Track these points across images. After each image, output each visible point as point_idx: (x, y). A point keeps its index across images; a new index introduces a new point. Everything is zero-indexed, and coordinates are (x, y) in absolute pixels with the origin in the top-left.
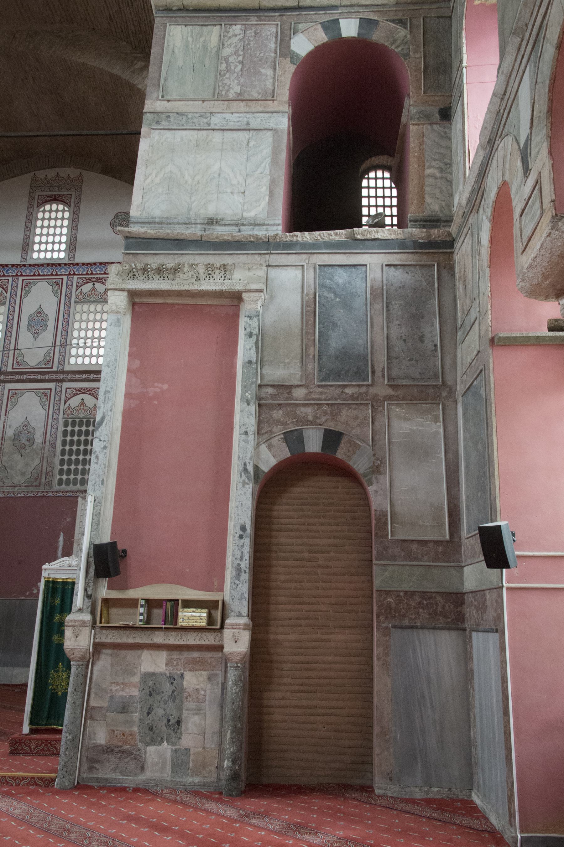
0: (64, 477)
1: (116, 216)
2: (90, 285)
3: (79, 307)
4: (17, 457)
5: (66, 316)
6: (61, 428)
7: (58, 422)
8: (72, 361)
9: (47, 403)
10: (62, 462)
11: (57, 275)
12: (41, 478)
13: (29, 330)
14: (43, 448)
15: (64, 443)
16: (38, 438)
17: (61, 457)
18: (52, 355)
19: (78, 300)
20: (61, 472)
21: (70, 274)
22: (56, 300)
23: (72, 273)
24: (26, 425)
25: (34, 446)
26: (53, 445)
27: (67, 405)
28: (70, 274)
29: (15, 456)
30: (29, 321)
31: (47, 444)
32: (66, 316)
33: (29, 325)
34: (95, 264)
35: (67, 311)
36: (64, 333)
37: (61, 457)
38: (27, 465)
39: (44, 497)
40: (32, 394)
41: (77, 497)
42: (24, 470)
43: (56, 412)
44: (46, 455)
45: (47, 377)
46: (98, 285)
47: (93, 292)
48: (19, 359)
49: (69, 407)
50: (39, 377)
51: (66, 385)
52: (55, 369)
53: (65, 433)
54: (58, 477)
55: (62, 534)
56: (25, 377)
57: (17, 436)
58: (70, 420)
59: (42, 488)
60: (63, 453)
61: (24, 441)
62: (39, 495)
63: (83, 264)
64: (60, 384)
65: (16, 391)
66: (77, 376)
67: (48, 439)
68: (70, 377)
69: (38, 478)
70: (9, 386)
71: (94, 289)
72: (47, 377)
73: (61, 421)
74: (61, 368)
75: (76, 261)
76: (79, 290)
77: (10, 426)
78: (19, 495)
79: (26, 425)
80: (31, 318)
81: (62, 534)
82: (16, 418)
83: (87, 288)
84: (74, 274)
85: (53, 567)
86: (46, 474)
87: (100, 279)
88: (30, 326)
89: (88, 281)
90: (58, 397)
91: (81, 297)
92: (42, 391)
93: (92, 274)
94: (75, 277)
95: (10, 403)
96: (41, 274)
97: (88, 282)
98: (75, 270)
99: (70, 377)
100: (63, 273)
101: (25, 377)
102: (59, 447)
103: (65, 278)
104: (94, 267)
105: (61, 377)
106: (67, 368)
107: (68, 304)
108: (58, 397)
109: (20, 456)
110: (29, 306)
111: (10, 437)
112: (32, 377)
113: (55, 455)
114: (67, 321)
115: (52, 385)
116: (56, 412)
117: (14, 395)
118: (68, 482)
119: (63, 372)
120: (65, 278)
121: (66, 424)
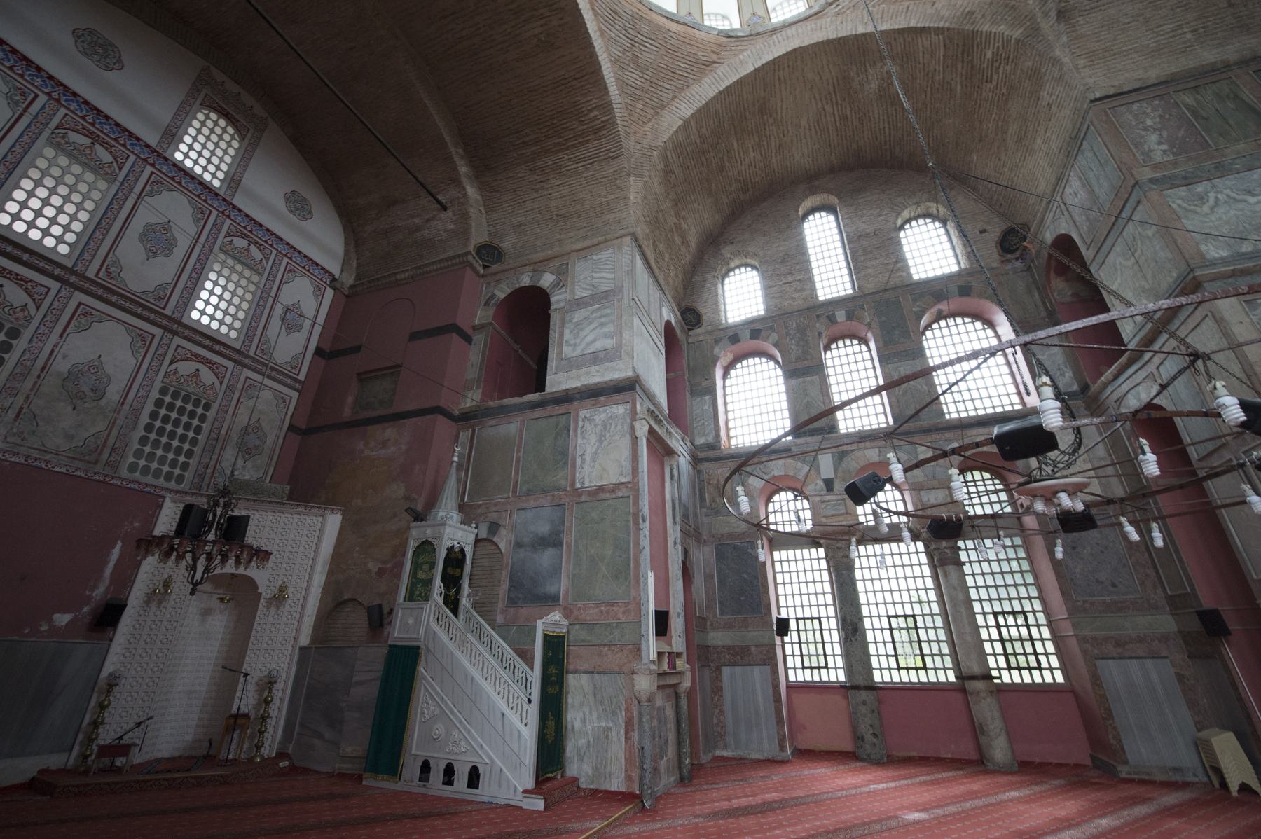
0: (142, 462)
1: (293, 192)
2: (245, 243)
6: (155, 394)
8: (195, 315)
9: (143, 351)
10: (144, 440)
11: (205, 201)
12: (100, 454)
15: (154, 415)
16: (113, 393)
17: (143, 433)
20: (139, 454)
21: (222, 212)
24: (96, 366)
26: (136, 413)
27: (173, 367)
28: (222, 212)
31: (126, 407)
34: (261, 225)
37: (143, 433)
39: (104, 482)
40: (122, 328)
45: (152, 316)
46: (253, 248)
49: (175, 371)
50: (139, 310)
51: (177, 340)
52: (168, 312)
53: (159, 403)
55: (119, 544)
56: (115, 299)
58: (172, 389)
59: (99, 468)
60: (149, 428)
61: (84, 388)
62: (96, 477)
63: (247, 216)
68: (187, 333)
70: (79, 296)
71: (248, 249)
73: (158, 384)
78: (57, 469)
79: (96, 366)
81: (119, 544)
83: (240, 243)
84: (229, 217)
86: (113, 449)
89: (243, 236)
90: (161, 351)
94: (228, 222)
95: (74, 322)
99: (187, 333)
102: (145, 419)
105: (175, 327)
106: (185, 320)
108: (161, 351)
109: (70, 408)
113: (135, 427)
115: (157, 331)
117: (82, 313)
118: (146, 471)
119: (179, 323)
120: (215, 213)
121: (163, 391)
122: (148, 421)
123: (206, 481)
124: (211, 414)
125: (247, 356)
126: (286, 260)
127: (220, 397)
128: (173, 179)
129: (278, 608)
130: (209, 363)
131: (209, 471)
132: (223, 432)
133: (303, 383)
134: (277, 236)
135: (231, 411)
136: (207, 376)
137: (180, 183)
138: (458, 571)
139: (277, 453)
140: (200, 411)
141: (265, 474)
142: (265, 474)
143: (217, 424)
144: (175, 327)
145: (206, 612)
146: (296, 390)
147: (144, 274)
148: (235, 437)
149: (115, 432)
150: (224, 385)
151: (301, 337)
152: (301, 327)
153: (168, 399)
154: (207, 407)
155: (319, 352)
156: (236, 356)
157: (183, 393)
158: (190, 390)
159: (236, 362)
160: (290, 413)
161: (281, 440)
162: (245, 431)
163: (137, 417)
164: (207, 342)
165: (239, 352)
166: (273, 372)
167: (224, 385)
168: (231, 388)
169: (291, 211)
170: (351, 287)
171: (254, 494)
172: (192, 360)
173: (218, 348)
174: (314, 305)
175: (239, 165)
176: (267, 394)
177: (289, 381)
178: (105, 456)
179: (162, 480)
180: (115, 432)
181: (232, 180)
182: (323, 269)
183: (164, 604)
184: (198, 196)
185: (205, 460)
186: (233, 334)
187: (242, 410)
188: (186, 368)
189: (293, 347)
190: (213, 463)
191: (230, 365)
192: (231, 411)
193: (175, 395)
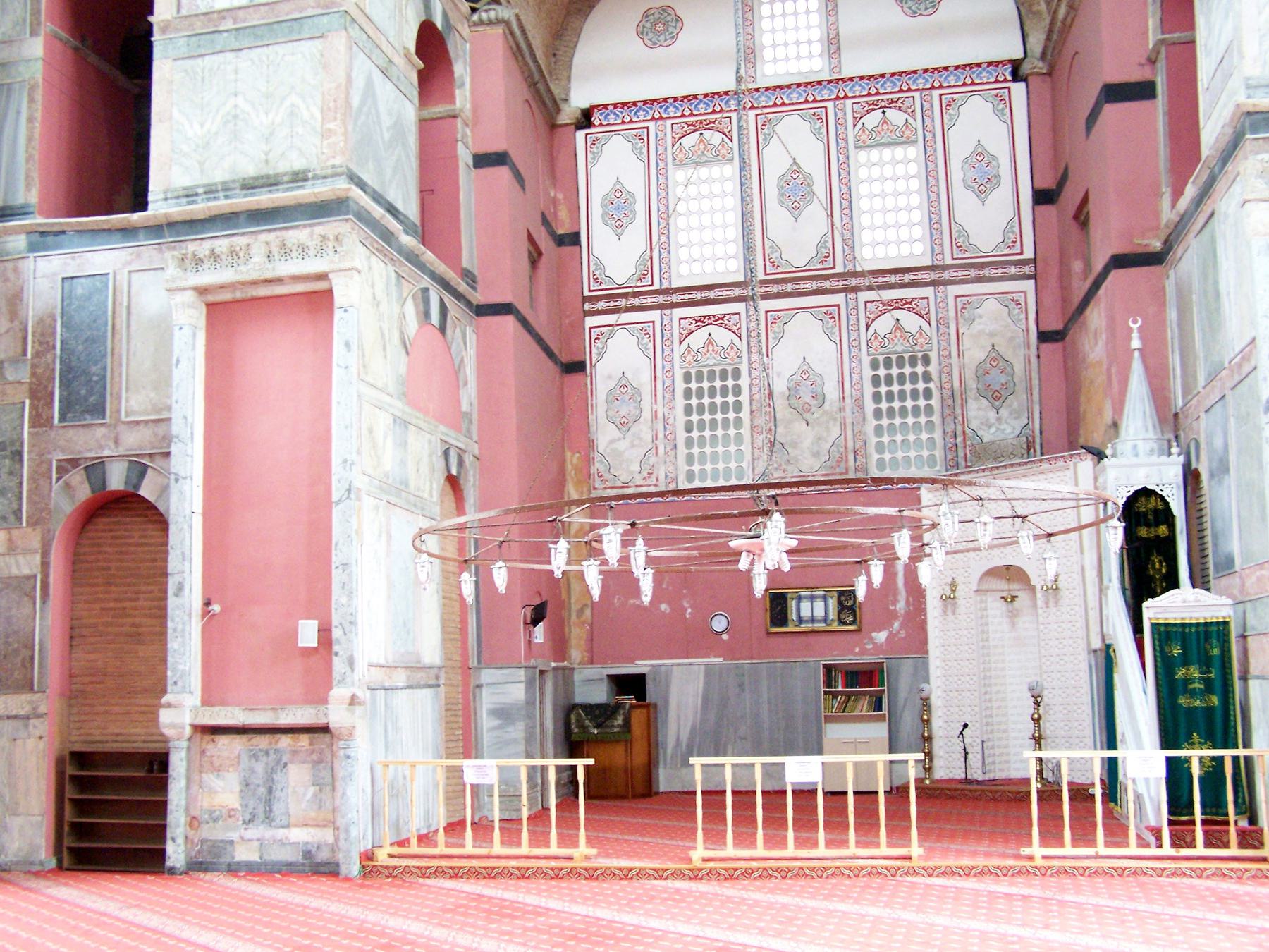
2: (878, 113)
3: (862, 156)
4: (800, 426)
5: (844, 174)
6: (868, 373)
7: (860, 361)
11: (815, 101)
12: (847, 461)
13: (782, 204)
14: (841, 409)
15: (877, 397)
16: (831, 391)
18: (830, 245)
19: (860, 144)
20: (880, 447)
21: (838, 98)
22: (821, 147)
23: (841, 95)
24: (805, 372)
25: (827, 406)
26: (859, 403)
27: (871, 331)
28: (838, 98)
29: (797, 424)
30: (780, 187)
31: (848, 400)
32: (844, 174)
33: (782, 195)
35: (845, 164)
36: (845, 204)
38: (819, 439)
41: (919, 488)
42: (815, 449)
43: (854, 344)
44: (849, 421)
45: (828, 284)
47: (885, 127)
48: (773, 256)
51: (864, 296)
53: (876, 381)
54: (876, 456)
57: (793, 391)
58: (881, 358)
60: (878, 414)
61: (807, 399)
64: (853, 296)
65: (780, 314)
66: (881, 279)
67: (847, 393)
69: (843, 459)
72: (828, 284)
73: (866, 360)
74: (850, 267)
75: (846, 74)
76: (859, 125)
77: (779, 375)
79: (805, 372)
80: (783, 182)
82: (784, 363)
83: (873, 119)
84: (846, 97)
85: (1159, 604)
87: (892, 102)
88: (783, 197)
89: (873, 107)
91: (864, 137)
92: (824, 310)
93: (878, 93)
94: (849, 102)
95: (771, 335)
96: (787, 101)
97: (872, 110)
98: (847, 90)
100: (826, 97)
101: (789, 288)
102: (870, 406)
103: (830, 105)
104: (882, 81)
105: (853, 282)
107: (843, 151)
110: (775, 163)
111: (783, 393)
112: (802, 286)
113: (864, 419)
114: (846, 181)
115: (839, 298)
116: (854, 344)
117: (774, 319)
119: (855, 274)
121: (875, 365)
122: (875, 406)
123: (961, 454)
124: (933, 368)
125: (944, 268)
126: (936, 93)
127: (935, 341)
128: (775, 105)
129: (1056, 603)
130: (905, 304)
131: (960, 439)
132: (956, 384)
133: (1034, 261)
134: (908, 73)
135: (954, 353)
136: (910, 322)
137: (783, 104)
138: (1163, 530)
139: (1035, 382)
140: (920, 369)
141: (1030, 418)
142: (1030, 418)
143: (945, 378)
144: (853, 282)
145: (1013, 616)
146: (1028, 277)
147: (797, 240)
148: (972, 384)
149: (849, 433)
150: (933, 323)
151: (1003, 195)
152: (997, 176)
153: (882, 372)
154: (926, 360)
155: (1043, 197)
156: (932, 276)
157: (894, 357)
158: (899, 348)
159: (934, 283)
160: (1032, 316)
161: (1034, 360)
162: (982, 372)
163: (862, 408)
164: (893, 279)
165: (932, 268)
166: (982, 269)
167: (933, 323)
168: (942, 323)
169: (914, 14)
170: (1043, 56)
171: (995, 459)
172: (882, 313)
173: (907, 278)
174: (1003, 129)
175: (828, 13)
176: (991, 305)
177: (1013, 270)
178: (851, 463)
179: (913, 468)
180: (849, 433)
181: (830, 43)
182: (990, 64)
183: (958, 611)
184: (806, 102)
185: (950, 428)
186: (918, 248)
187: (966, 343)
188: (884, 325)
189: (995, 218)
190: (959, 428)
191: (928, 291)
192: (954, 353)
193: (888, 363)
